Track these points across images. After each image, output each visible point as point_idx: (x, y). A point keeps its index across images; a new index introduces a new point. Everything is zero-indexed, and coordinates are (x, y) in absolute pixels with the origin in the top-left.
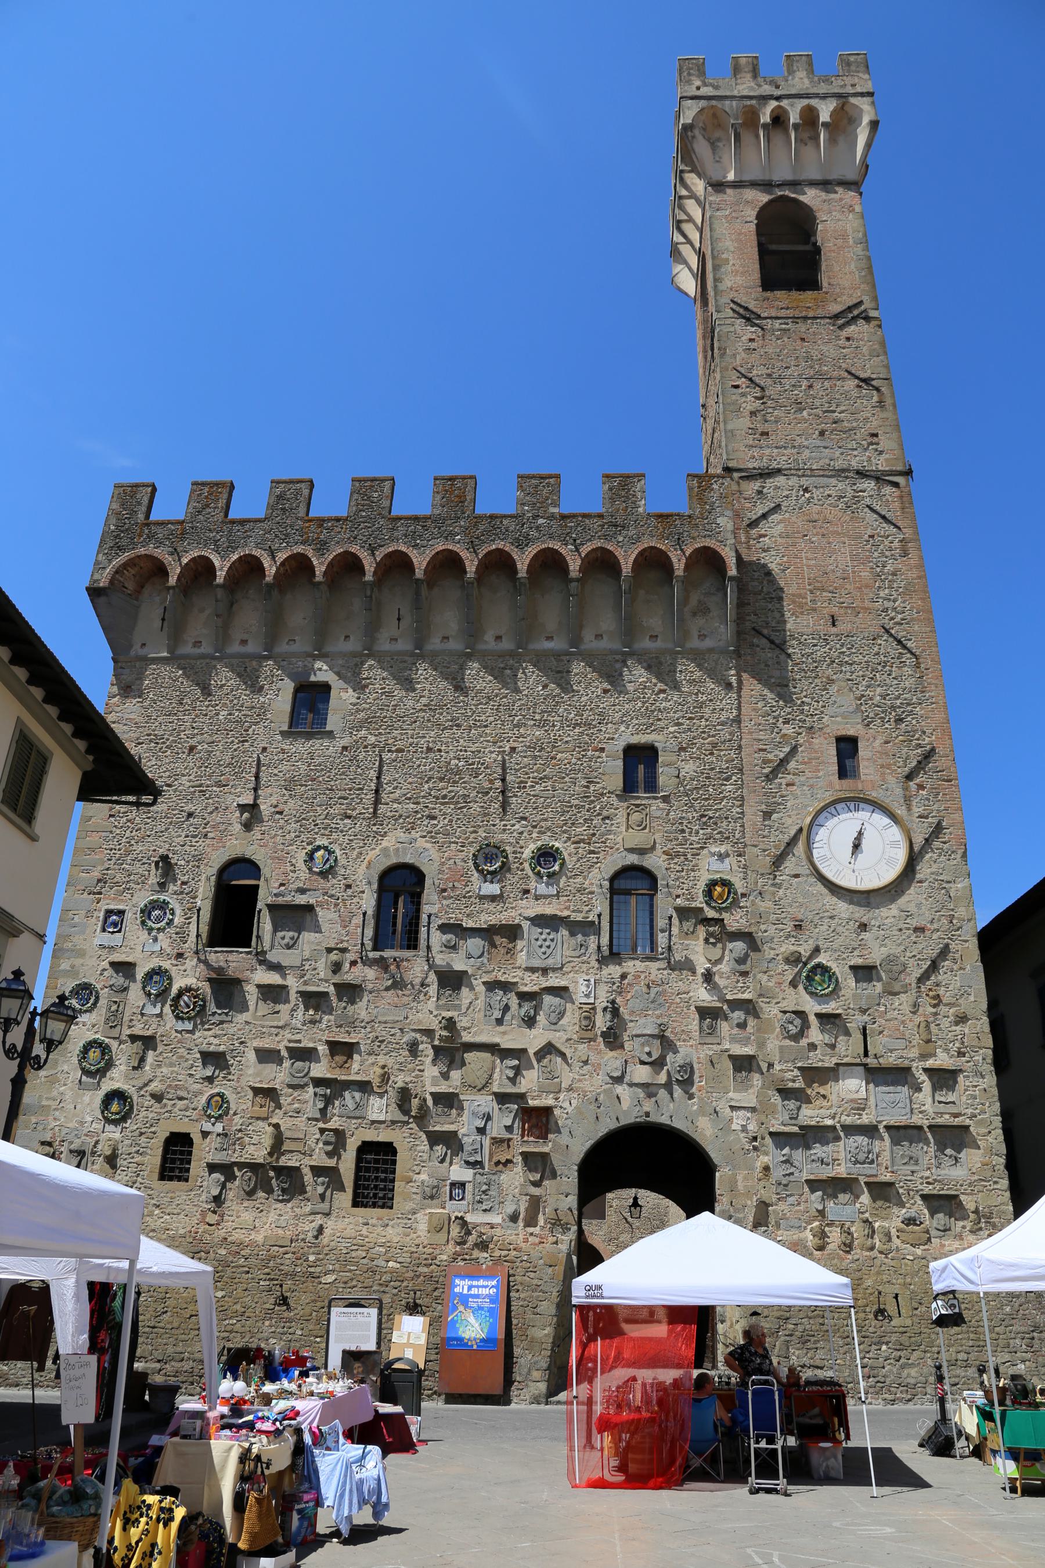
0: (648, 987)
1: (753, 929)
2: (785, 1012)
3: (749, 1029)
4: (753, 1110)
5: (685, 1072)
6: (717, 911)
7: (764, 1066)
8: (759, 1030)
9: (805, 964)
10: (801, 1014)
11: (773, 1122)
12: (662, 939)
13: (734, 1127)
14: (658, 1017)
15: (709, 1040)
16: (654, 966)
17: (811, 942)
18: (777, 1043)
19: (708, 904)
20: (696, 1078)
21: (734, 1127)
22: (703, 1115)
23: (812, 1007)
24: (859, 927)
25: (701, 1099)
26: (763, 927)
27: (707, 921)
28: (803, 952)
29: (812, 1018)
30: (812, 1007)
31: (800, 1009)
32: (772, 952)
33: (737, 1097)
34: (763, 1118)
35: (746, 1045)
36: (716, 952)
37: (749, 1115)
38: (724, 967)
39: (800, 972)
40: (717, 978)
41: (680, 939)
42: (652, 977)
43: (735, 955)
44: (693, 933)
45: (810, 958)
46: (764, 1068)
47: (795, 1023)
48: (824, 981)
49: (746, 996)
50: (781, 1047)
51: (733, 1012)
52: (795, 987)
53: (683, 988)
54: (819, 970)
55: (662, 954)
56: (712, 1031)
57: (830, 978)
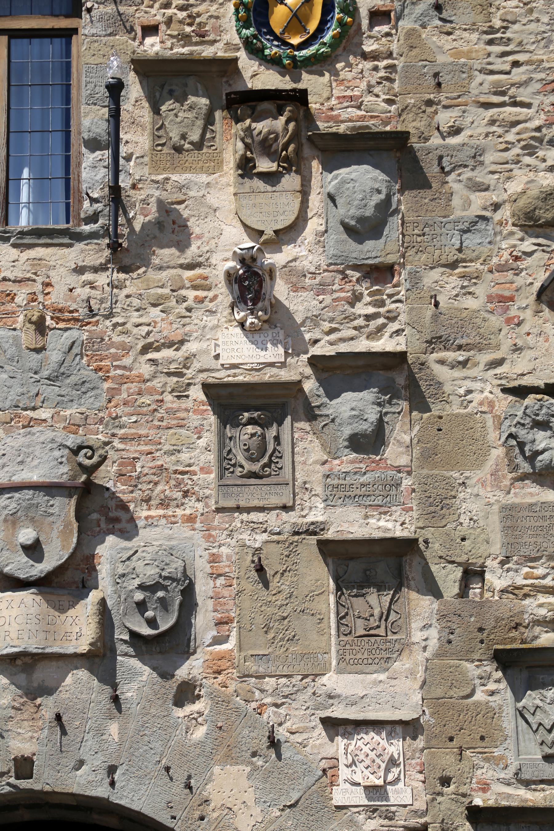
0: (40, 327)
1: (411, 125)
2: (520, 392)
3: (395, 453)
4: (409, 728)
5: (164, 604)
6: (283, 70)
7: (449, 578)
8: (429, 456)
11: (486, 772)
12: (92, 171)
13: (341, 795)
14: (73, 427)
15: (253, 495)
16: (60, 260)
18: (497, 497)
19: (254, 50)
20: (203, 623)
21: (341, 795)
22: (230, 758)
25: (220, 701)
26: (445, 118)
27: (247, 103)
32: (478, 200)
33: (350, 688)
34: (447, 761)
35: (383, 510)
36: (276, 206)
37: (395, 747)
38: (302, 253)
40: (280, 290)
41: (156, 167)
42: (57, 296)
43: (348, 211)
44: (199, 146)
46: (449, 578)
49: (385, 344)
50: (509, 513)
51: (332, 395)
53: (166, 329)
55: (93, 218)
56: (265, 464)
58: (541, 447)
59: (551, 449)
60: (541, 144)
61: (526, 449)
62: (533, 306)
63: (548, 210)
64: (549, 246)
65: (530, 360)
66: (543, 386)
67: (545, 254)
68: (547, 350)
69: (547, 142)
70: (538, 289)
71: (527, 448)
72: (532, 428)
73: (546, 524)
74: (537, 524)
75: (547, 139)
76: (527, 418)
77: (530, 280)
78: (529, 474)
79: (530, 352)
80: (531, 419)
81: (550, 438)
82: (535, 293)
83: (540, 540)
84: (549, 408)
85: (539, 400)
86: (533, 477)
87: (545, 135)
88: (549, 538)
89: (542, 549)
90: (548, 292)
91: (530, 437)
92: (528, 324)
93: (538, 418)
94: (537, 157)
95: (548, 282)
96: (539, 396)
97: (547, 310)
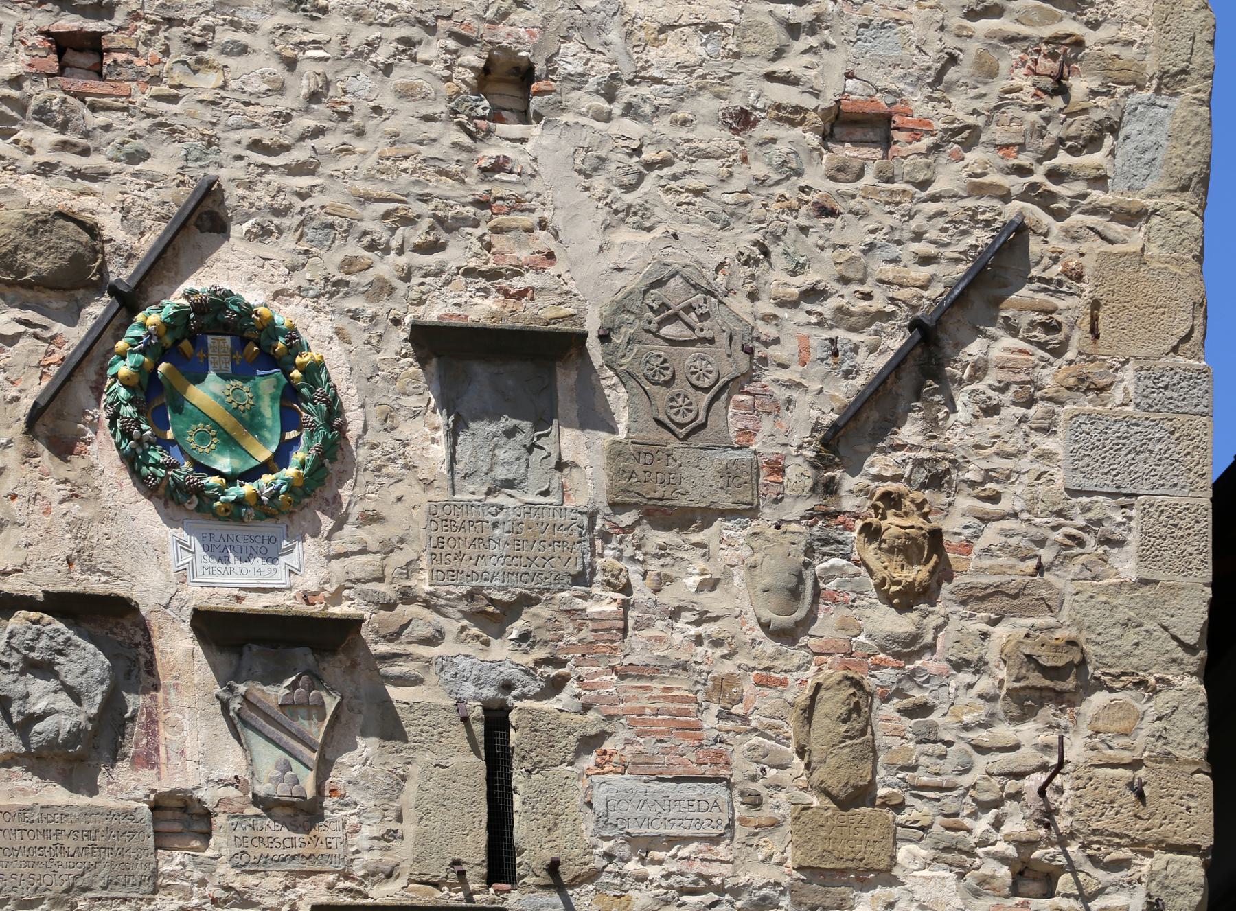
9: (129, 302)
10: (106, 617)
17: (165, 160)
23: (170, 571)
24: (486, 76)
28: (111, 226)
29: (177, 648)
30: (170, 571)
31: (95, 584)
39: (88, 363)
45: (165, 263)
47: (69, 669)
48: (252, 422)
52: (64, 447)
54: (220, 344)
57: (290, 396)
58: (39, 707)
59: (57, 712)
60: (24, 116)
61: (12, 709)
62: (20, 445)
63: (40, 254)
64: (46, 328)
65: (17, 547)
66: (41, 597)
67: (39, 343)
68: (47, 530)
69: (35, 112)
70: (28, 411)
71: (14, 709)
72: (23, 673)
73: (49, 844)
74: (34, 843)
75: (33, 105)
76: (15, 654)
77: (12, 393)
78: (19, 755)
79: (16, 531)
80: (20, 656)
81: (55, 692)
82: (24, 419)
83: (39, 871)
84: (52, 638)
85: (35, 622)
86: (27, 761)
87: (30, 96)
88: (55, 868)
89: (44, 886)
90: (47, 418)
91: (19, 688)
92: (11, 478)
93: (32, 655)
94: (16, 142)
95: (46, 399)
96: (35, 615)
97: (47, 453)
